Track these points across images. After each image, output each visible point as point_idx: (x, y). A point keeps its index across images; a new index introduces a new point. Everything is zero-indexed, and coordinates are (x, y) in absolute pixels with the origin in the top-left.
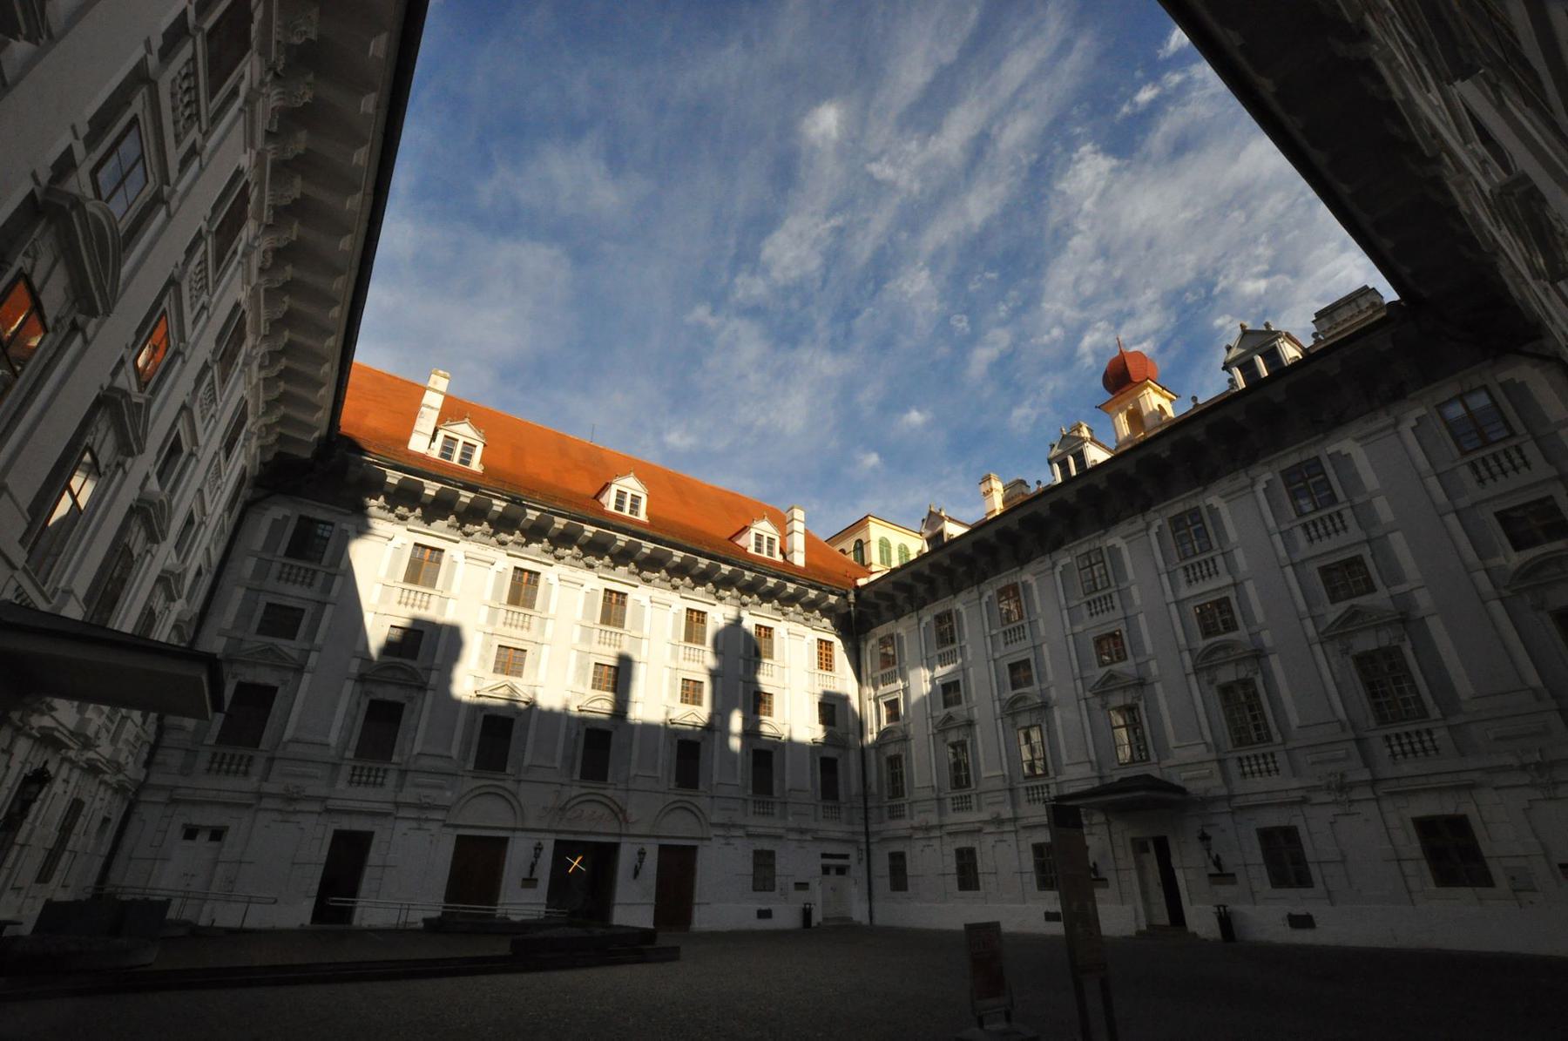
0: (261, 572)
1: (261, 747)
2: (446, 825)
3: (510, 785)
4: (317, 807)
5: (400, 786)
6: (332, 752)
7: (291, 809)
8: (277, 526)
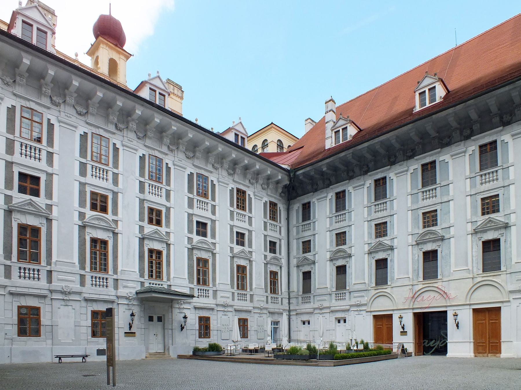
0: (298, 233)
1: (312, 293)
4: (328, 311)
5: (350, 299)
6: (329, 290)
7: (321, 312)
8: (297, 211)
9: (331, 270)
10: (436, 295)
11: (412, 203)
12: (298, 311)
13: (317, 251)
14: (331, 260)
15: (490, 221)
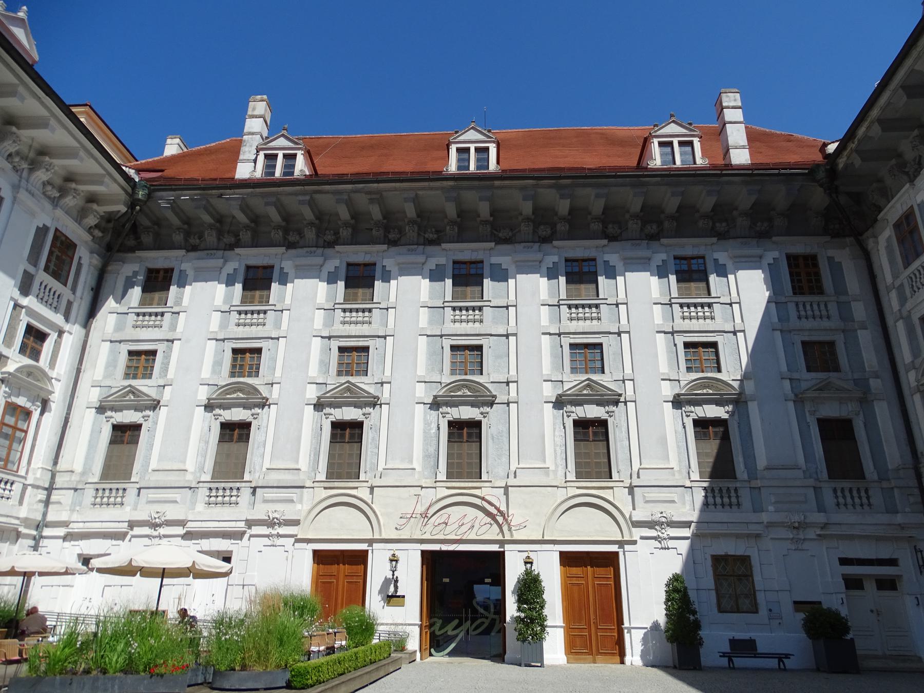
1: (133, 480)
2: (298, 541)
3: (364, 493)
4: (180, 531)
7: (155, 533)
9: (207, 428)
10: (481, 515)
11: (431, 322)
12: (71, 525)
13: (172, 380)
14: (209, 407)
15: (588, 385)
